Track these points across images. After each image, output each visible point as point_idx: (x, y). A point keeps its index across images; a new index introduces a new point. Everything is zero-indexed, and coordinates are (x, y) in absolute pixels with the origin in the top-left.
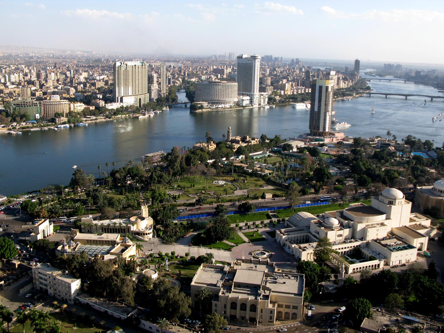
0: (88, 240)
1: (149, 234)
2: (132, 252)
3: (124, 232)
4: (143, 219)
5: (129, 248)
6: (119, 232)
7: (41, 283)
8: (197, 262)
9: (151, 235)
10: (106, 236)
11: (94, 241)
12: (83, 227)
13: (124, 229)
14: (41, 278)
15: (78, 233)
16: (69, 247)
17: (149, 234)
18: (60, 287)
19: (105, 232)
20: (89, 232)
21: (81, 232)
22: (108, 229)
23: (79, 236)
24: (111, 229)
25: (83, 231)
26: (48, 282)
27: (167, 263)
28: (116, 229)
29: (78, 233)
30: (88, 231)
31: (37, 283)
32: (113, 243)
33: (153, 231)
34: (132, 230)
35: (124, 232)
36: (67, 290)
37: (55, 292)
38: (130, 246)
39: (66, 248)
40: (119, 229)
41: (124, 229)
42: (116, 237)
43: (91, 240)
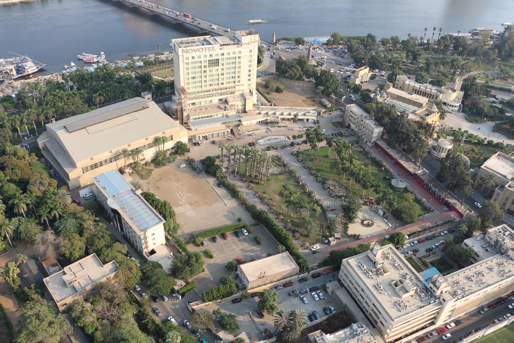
0: (398, 96)
1: (455, 106)
2: (433, 119)
3: (433, 98)
4: (455, 91)
5: (433, 114)
6: (428, 97)
7: (350, 120)
8: (493, 148)
9: (457, 109)
10: (415, 97)
11: (403, 98)
12: (396, 82)
13: (433, 95)
14: (352, 117)
15: (391, 87)
16: (381, 96)
17: (455, 106)
18: (365, 128)
19: (415, 93)
20: (401, 89)
21: (394, 87)
22: (418, 91)
23: (392, 90)
24: (421, 92)
25: (396, 86)
26: (356, 121)
27: (464, 139)
28: (426, 93)
29: (391, 87)
30: (400, 88)
31: (347, 119)
32: (420, 105)
33: (460, 105)
34: (440, 98)
35: (433, 98)
36: (370, 133)
37: (360, 131)
38: (434, 112)
39: (378, 97)
40: (428, 94)
41: (433, 95)
42: (423, 100)
43: (401, 97)
